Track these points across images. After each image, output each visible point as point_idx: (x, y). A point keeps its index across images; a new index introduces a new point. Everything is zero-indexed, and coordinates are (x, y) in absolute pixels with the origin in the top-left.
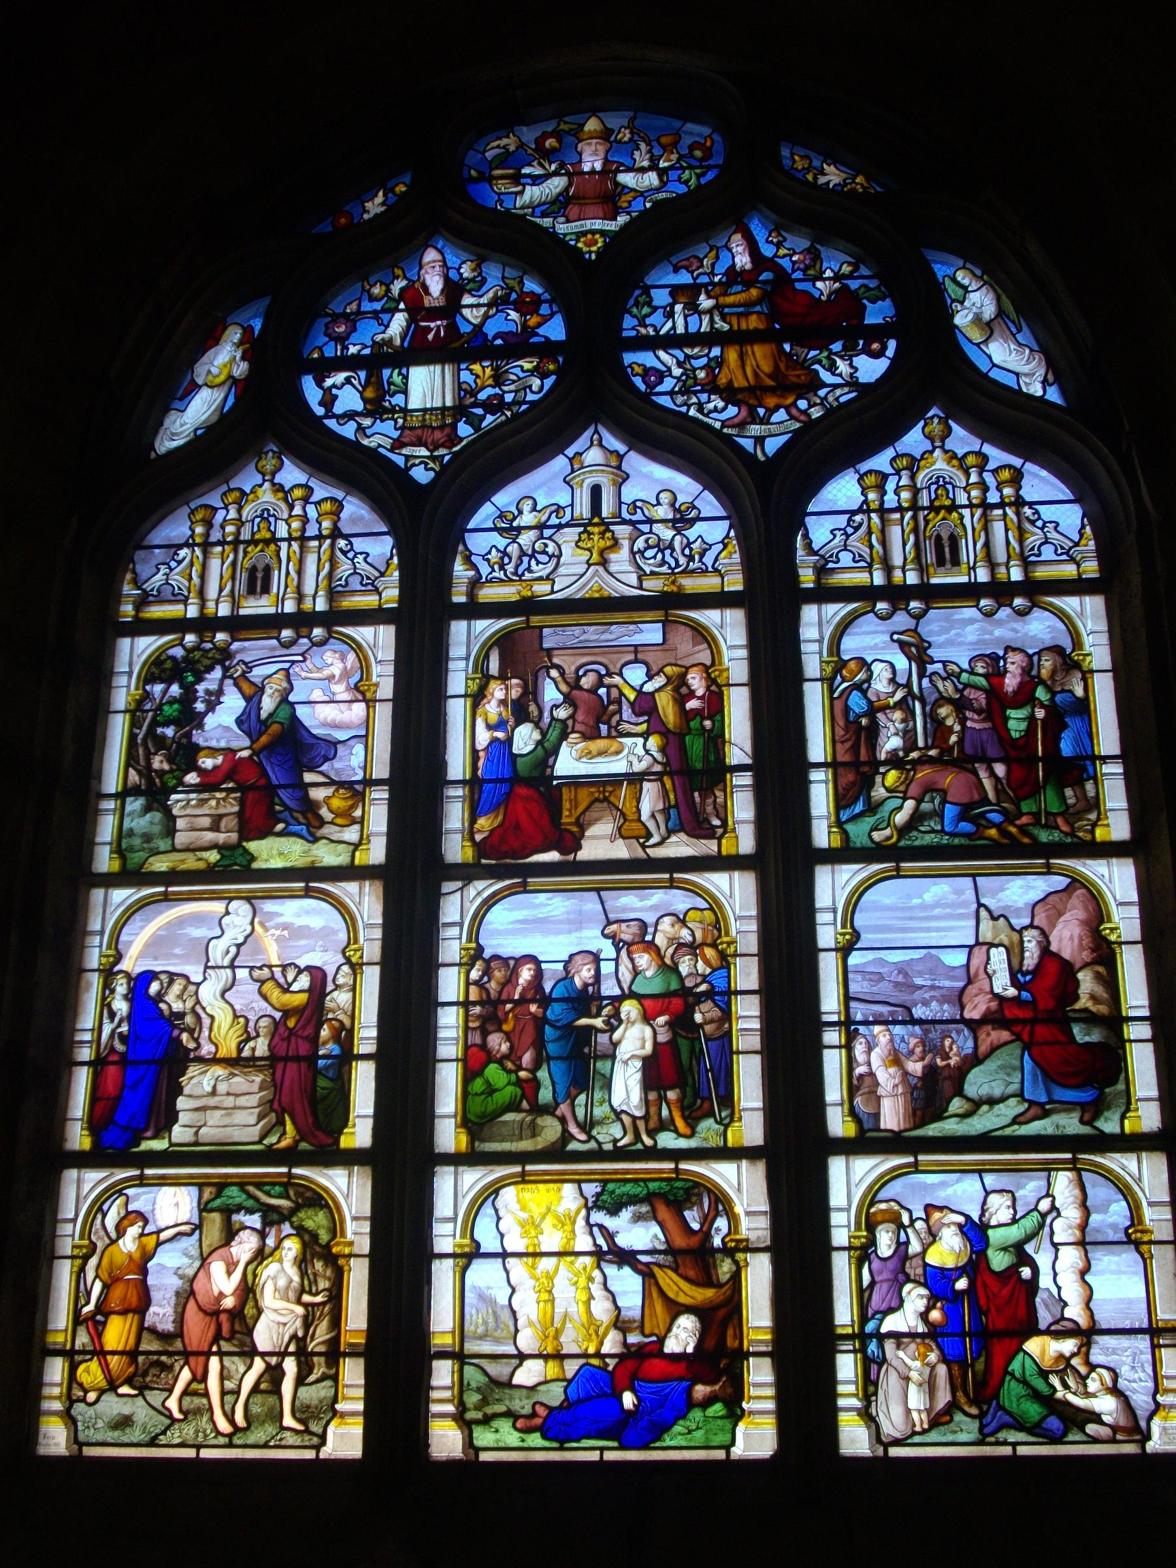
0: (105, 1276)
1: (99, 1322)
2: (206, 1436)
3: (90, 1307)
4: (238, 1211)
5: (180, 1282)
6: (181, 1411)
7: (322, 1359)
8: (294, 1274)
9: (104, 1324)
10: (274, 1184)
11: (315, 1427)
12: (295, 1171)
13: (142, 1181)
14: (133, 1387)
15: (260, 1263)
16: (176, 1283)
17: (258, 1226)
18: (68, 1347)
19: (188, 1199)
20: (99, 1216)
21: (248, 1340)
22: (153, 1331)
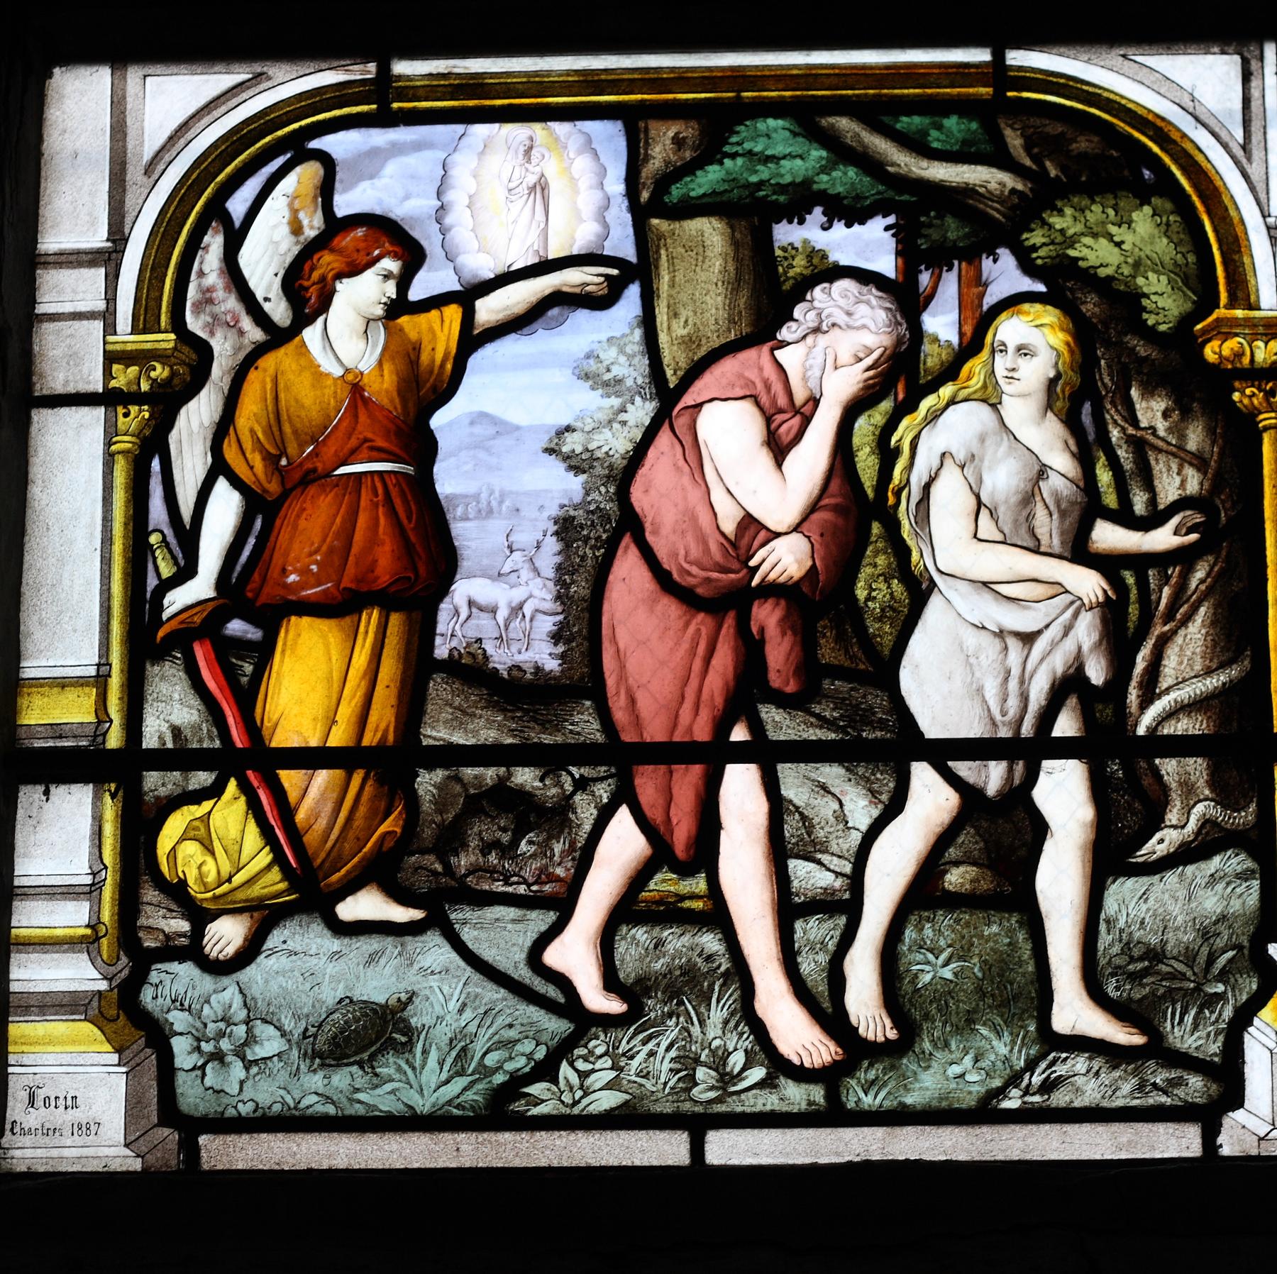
0: (252, 466)
1: (240, 645)
2: (726, 1079)
3: (200, 587)
4: (797, 213)
5: (574, 485)
6: (611, 982)
7: (1196, 767)
8: (1050, 443)
9: (264, 653)
10: (937, 108)
11: (1192, 1036)
12: (1015, 58)
13: (385, 106)
14: (401, 896)
15: (907, 407)
16: (565, 487)
17: (886, 264)
18: (114, 740)
19: (582, 165)
20: (214, 243)
21: (877, 700)
22: (471, 671)
